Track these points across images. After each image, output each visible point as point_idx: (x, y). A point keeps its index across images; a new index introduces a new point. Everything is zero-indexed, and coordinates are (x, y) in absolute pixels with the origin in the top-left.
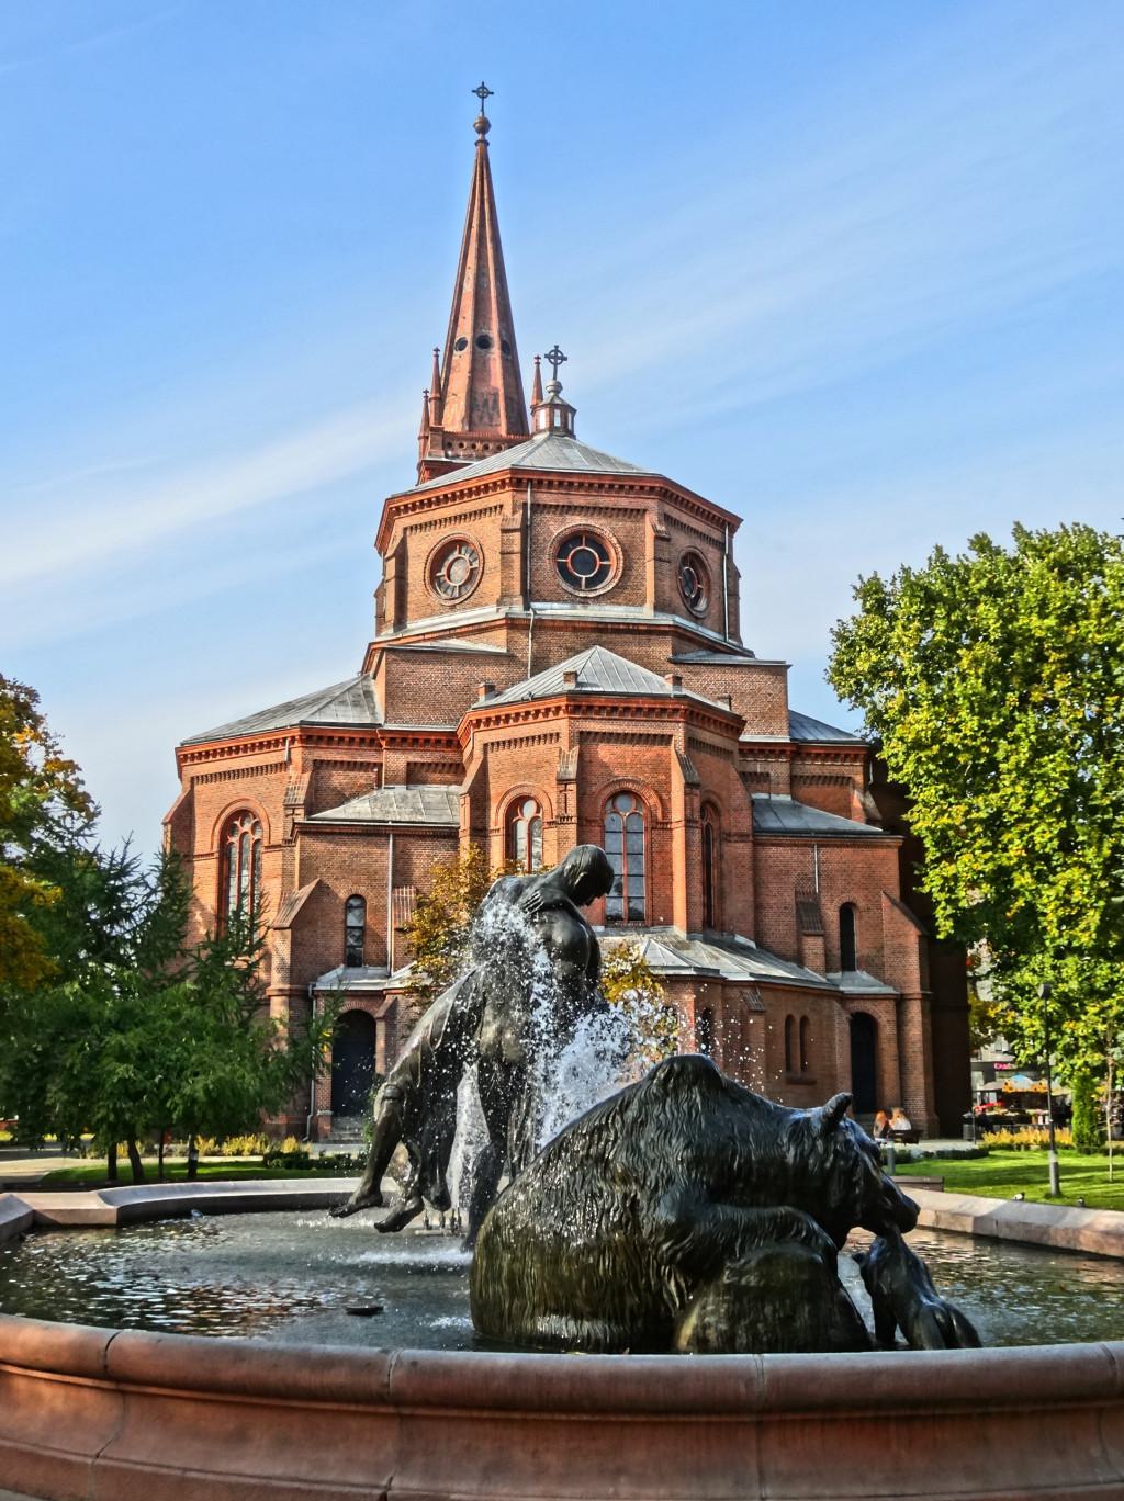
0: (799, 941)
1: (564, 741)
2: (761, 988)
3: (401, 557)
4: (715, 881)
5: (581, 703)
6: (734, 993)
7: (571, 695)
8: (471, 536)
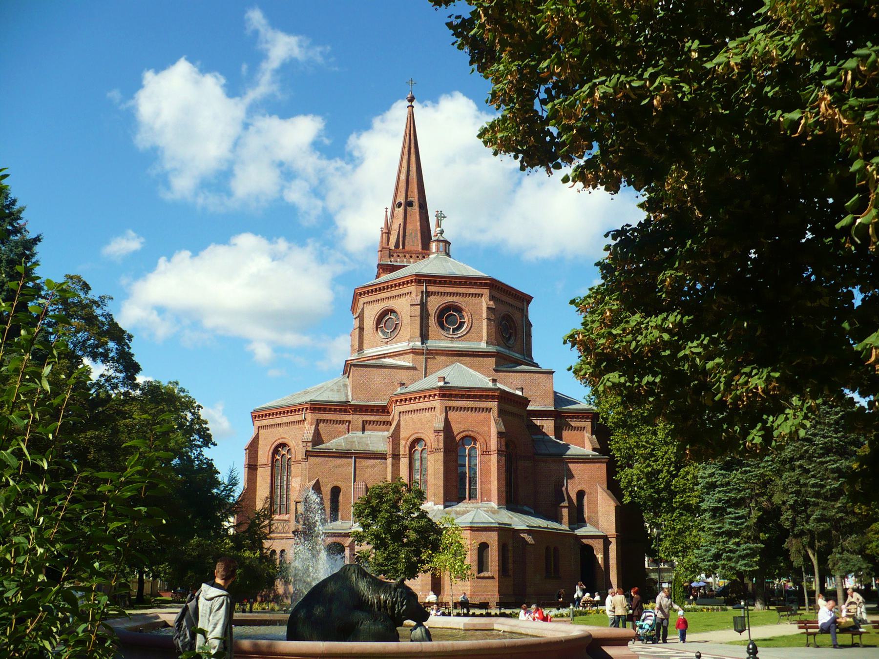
1: (438, 410)
3: (361, 317)
5: (446, 392)
7: (441, 388)
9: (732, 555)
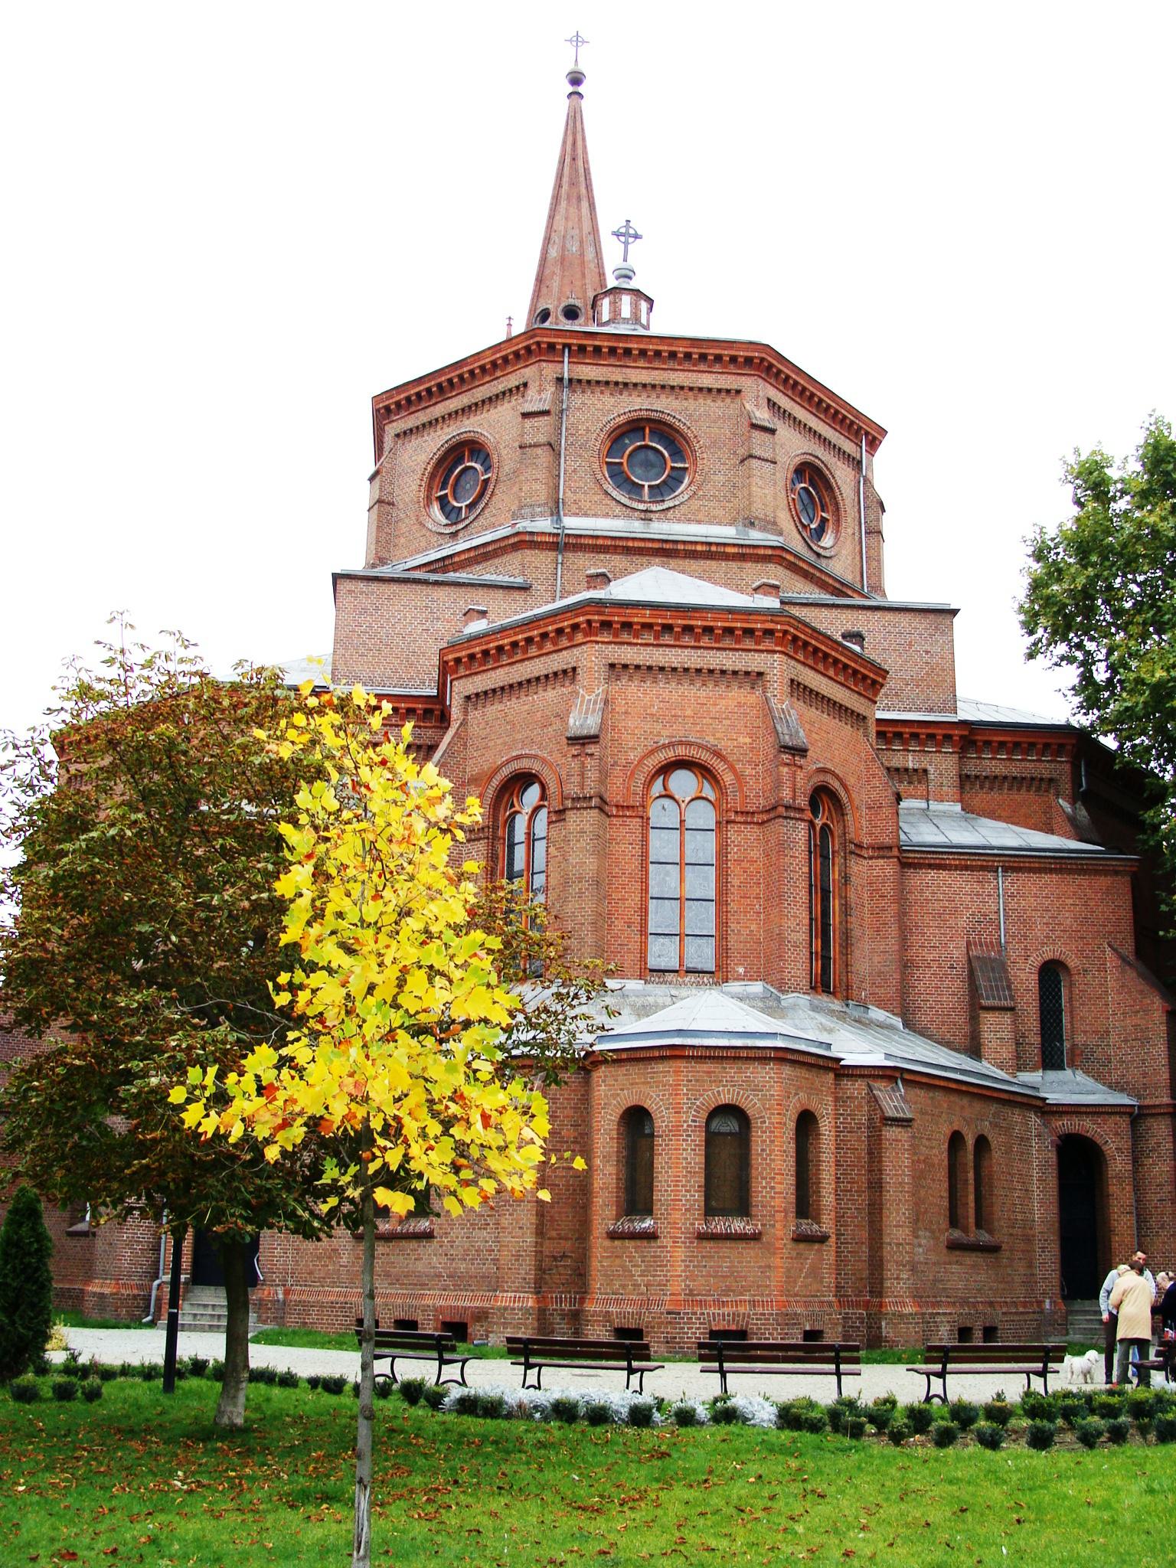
0: (974, 1020)
2: (904, 1081)
4: (835, 919)
6: (856, 1088)
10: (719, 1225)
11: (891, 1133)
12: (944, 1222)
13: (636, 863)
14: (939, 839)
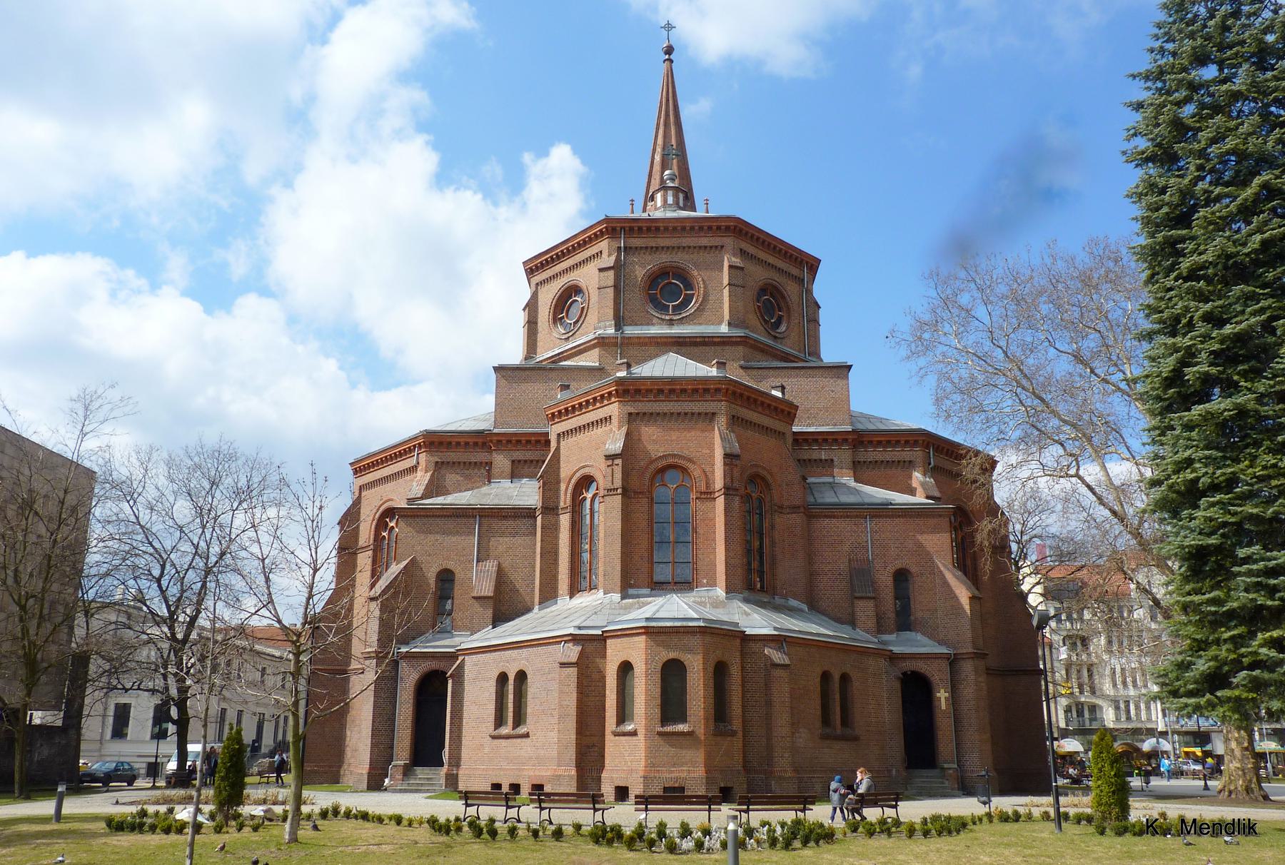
5: (629, 390)
8: (583, 284)
9: (1266, 675)
10: (669, 729)
11: (777, 673)
12: (818, 724)
13: (645, 523)
14: (835, 500)
